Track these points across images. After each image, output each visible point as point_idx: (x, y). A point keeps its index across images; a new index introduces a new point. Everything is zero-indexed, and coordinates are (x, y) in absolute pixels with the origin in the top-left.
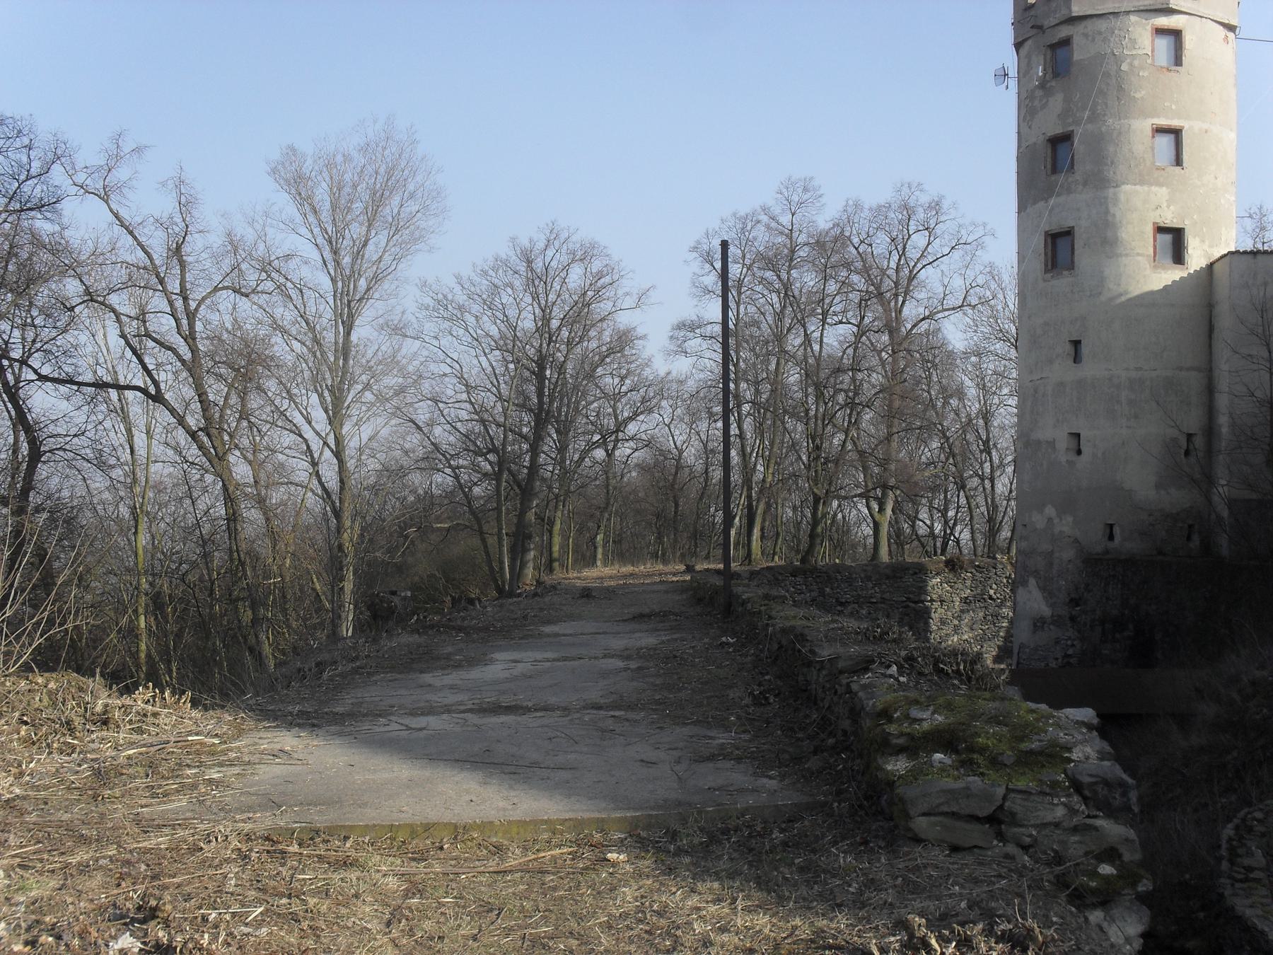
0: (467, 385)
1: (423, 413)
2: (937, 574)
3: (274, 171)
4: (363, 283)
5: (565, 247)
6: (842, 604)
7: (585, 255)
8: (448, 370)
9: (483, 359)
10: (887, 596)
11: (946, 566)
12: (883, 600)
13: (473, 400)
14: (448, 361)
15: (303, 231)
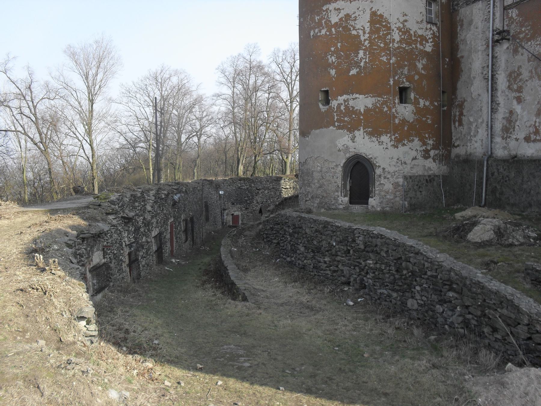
0: (138, 118)
1: (124, 129)
2: (292, 179)
3: (65, 52)
4: (97, 87)
5: (168, 72)
6: (258, 190)
7: (176, 73)
8: (132, 114)
9: (142, 110)
10: (275, 187)
11: (295, 176)
12: (273, 188)
13: (140, 124)
14: (132, 111)
15: (76, 71)
